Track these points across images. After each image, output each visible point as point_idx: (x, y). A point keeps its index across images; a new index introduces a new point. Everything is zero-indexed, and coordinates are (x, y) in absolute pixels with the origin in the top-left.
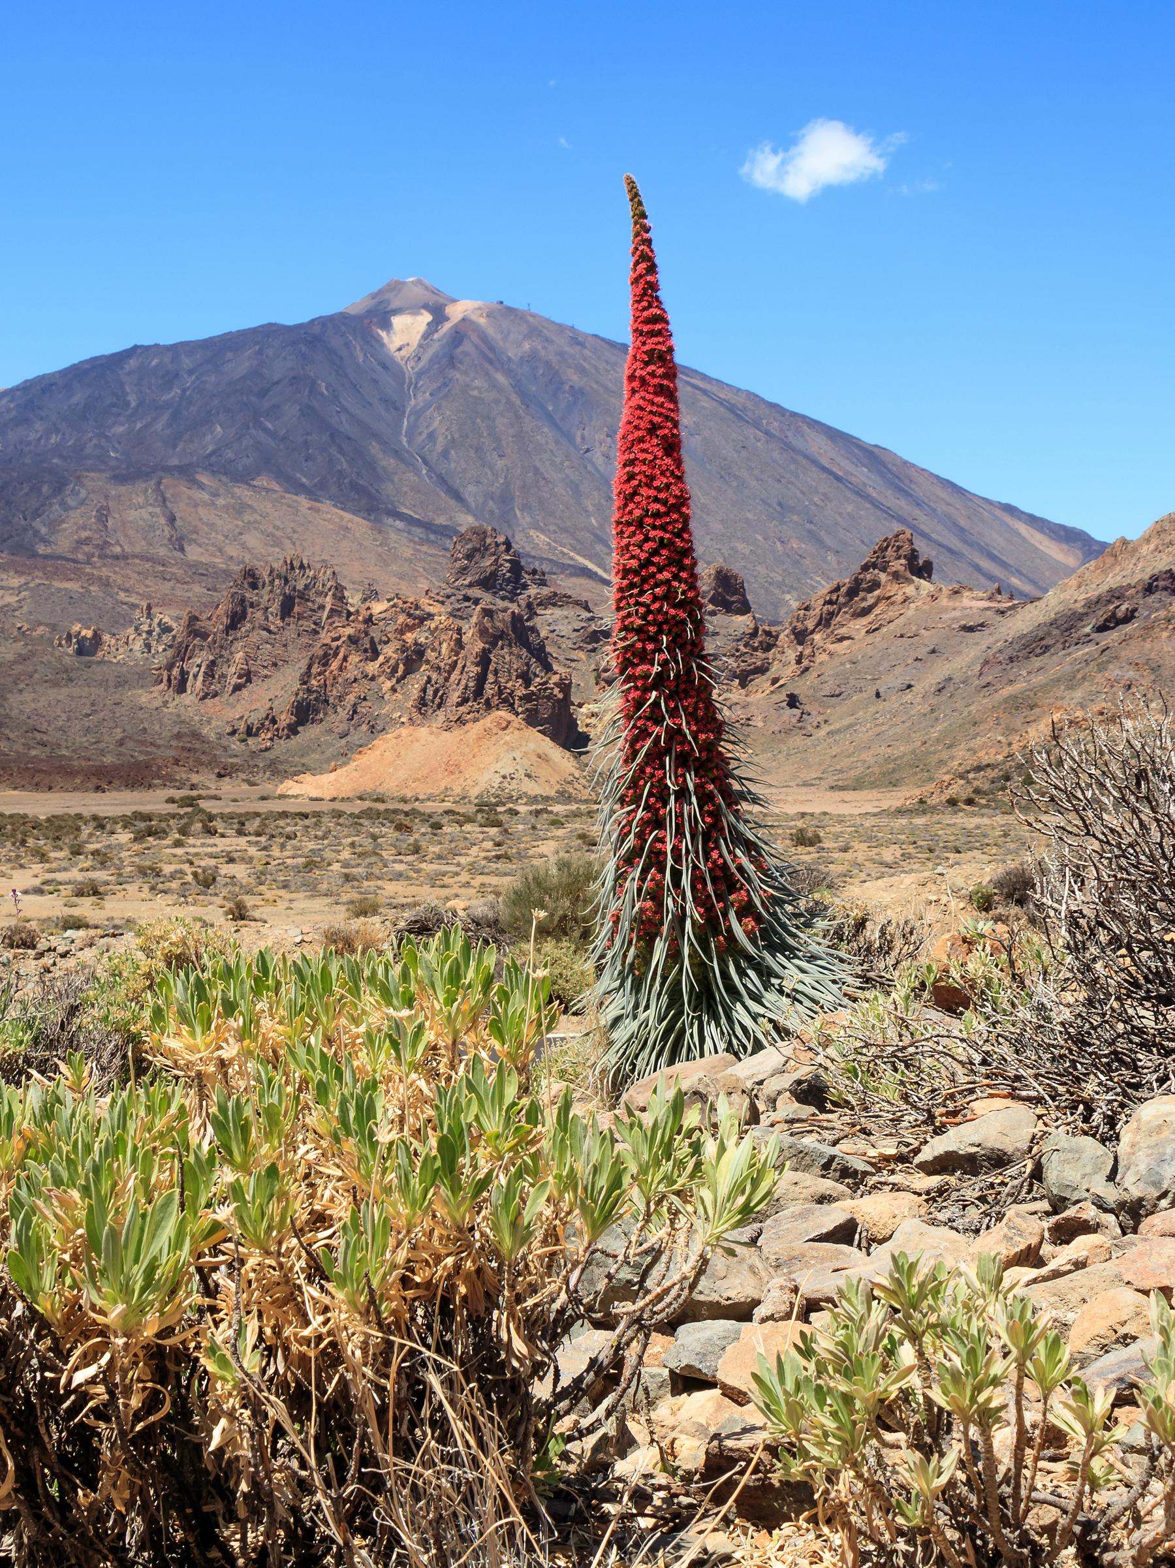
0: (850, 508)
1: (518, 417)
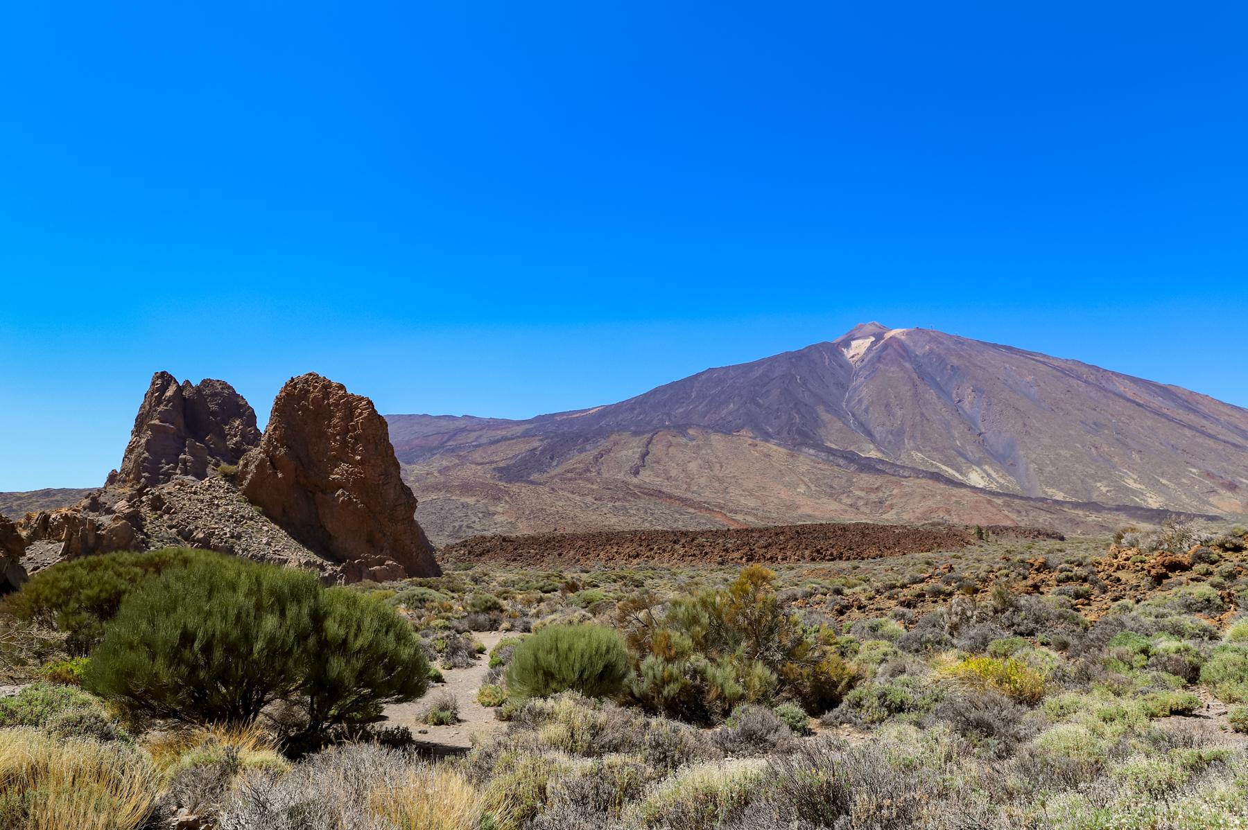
0: (1149, 423)
1: (915, 385)
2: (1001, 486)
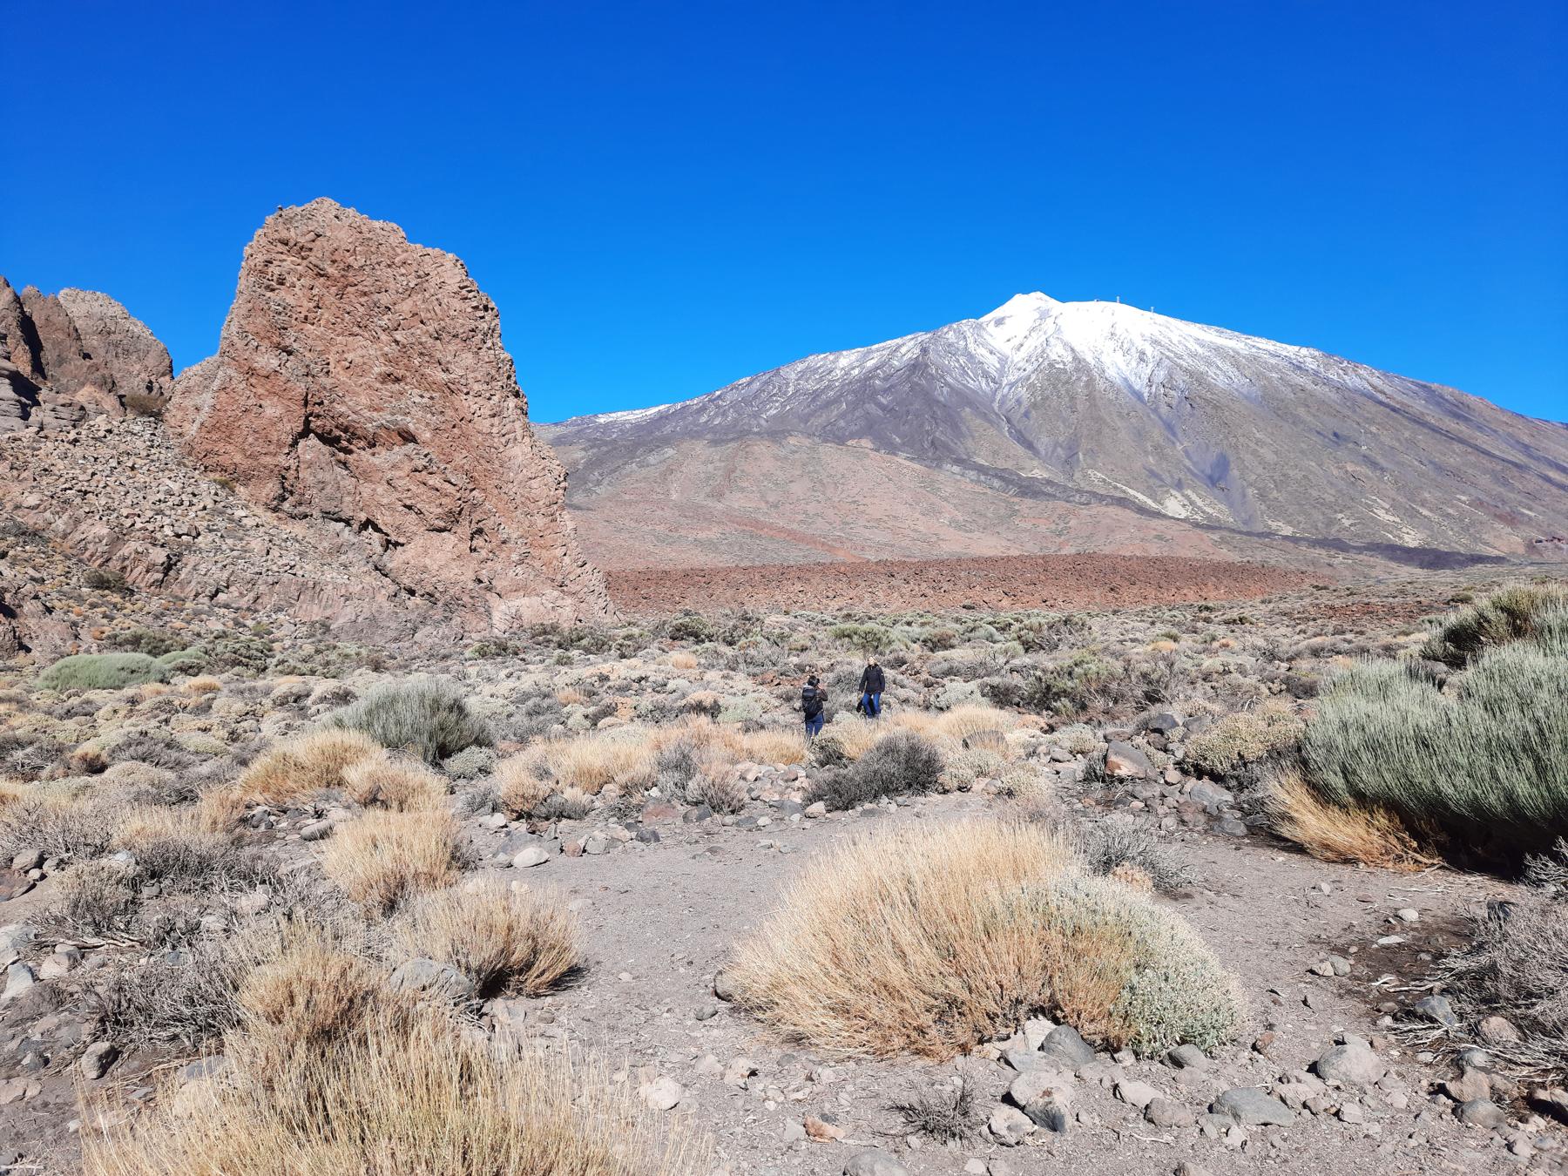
0: (1407, 434)
2: (1209, 517)
